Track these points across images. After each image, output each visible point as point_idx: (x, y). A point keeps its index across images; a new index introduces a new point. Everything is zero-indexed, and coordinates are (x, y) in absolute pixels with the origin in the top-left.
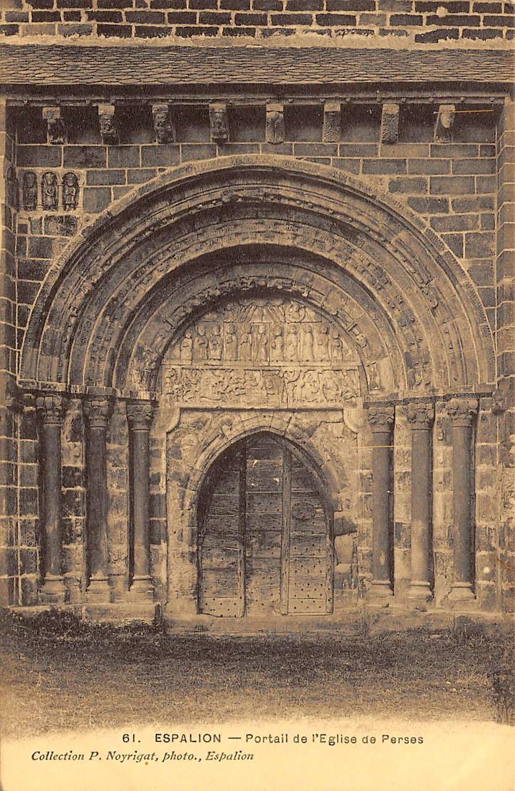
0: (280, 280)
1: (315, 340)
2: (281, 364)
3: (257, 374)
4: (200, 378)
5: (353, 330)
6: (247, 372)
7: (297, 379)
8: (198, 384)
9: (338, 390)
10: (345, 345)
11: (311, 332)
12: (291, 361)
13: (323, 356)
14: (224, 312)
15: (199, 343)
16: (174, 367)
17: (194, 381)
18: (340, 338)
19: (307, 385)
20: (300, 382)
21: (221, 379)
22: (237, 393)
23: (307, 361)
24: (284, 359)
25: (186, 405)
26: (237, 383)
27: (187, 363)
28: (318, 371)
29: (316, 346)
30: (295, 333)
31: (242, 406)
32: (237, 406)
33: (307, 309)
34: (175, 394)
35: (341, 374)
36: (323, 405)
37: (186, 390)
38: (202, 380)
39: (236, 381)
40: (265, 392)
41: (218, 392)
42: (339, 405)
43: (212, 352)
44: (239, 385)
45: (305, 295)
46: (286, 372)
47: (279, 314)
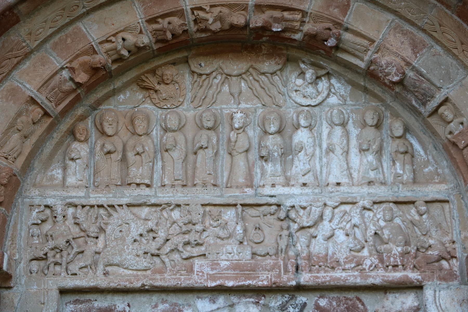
0: (277, 14)
1: (354, 142)
2: (280, 190)
3: (229, 215)
4: (106, 224)
5: (441, 110)
6: (208, 208)
7: (315, 224)
8: (102, 238)
9: (407, 243)
10: (417, 146)
11: (343, 125)
12: (304, 185)
13: (372, 175)
14: (158, 87)
15: (105, 150)
16: (49, 202)
17: (93, 230)
18: (408, 136)
19: (340, 236)
20: (326, 227)
21: (150, 224)
22: (186, 255)
23: (338, 184)
24: (287, 184)
25: (71, 283)
26: (188, 232)
27: (78, 195)
28: (361, 203)
29: (354, 151)
30: (310, 127)
31: (196, 280)
32: (184, 281)
33: (333, 81)
34: (51, 260)
35: (413, 211)
36: (378, 277)
37: (75, 250)
38: (109, 229)
39: (184, 229)
40: (247, 254)
41: (146, 253)
42: (414, 276)
43: (133, 170)
44: (191, 237)
45: (331, 42)
46: (293, 207)
47: (274, 92)
